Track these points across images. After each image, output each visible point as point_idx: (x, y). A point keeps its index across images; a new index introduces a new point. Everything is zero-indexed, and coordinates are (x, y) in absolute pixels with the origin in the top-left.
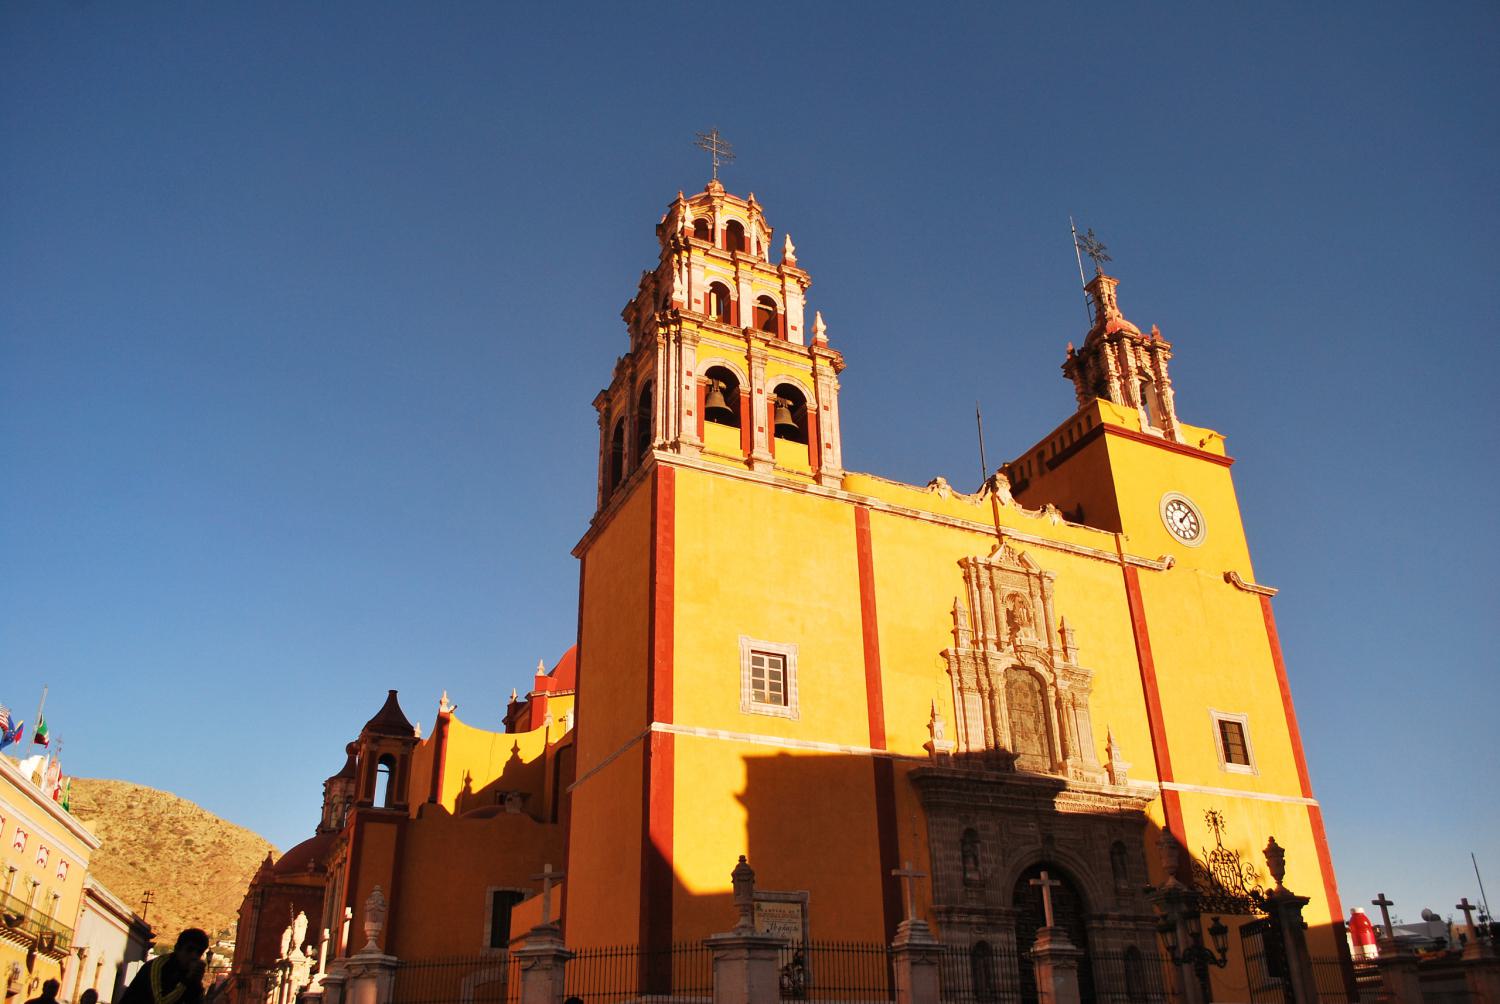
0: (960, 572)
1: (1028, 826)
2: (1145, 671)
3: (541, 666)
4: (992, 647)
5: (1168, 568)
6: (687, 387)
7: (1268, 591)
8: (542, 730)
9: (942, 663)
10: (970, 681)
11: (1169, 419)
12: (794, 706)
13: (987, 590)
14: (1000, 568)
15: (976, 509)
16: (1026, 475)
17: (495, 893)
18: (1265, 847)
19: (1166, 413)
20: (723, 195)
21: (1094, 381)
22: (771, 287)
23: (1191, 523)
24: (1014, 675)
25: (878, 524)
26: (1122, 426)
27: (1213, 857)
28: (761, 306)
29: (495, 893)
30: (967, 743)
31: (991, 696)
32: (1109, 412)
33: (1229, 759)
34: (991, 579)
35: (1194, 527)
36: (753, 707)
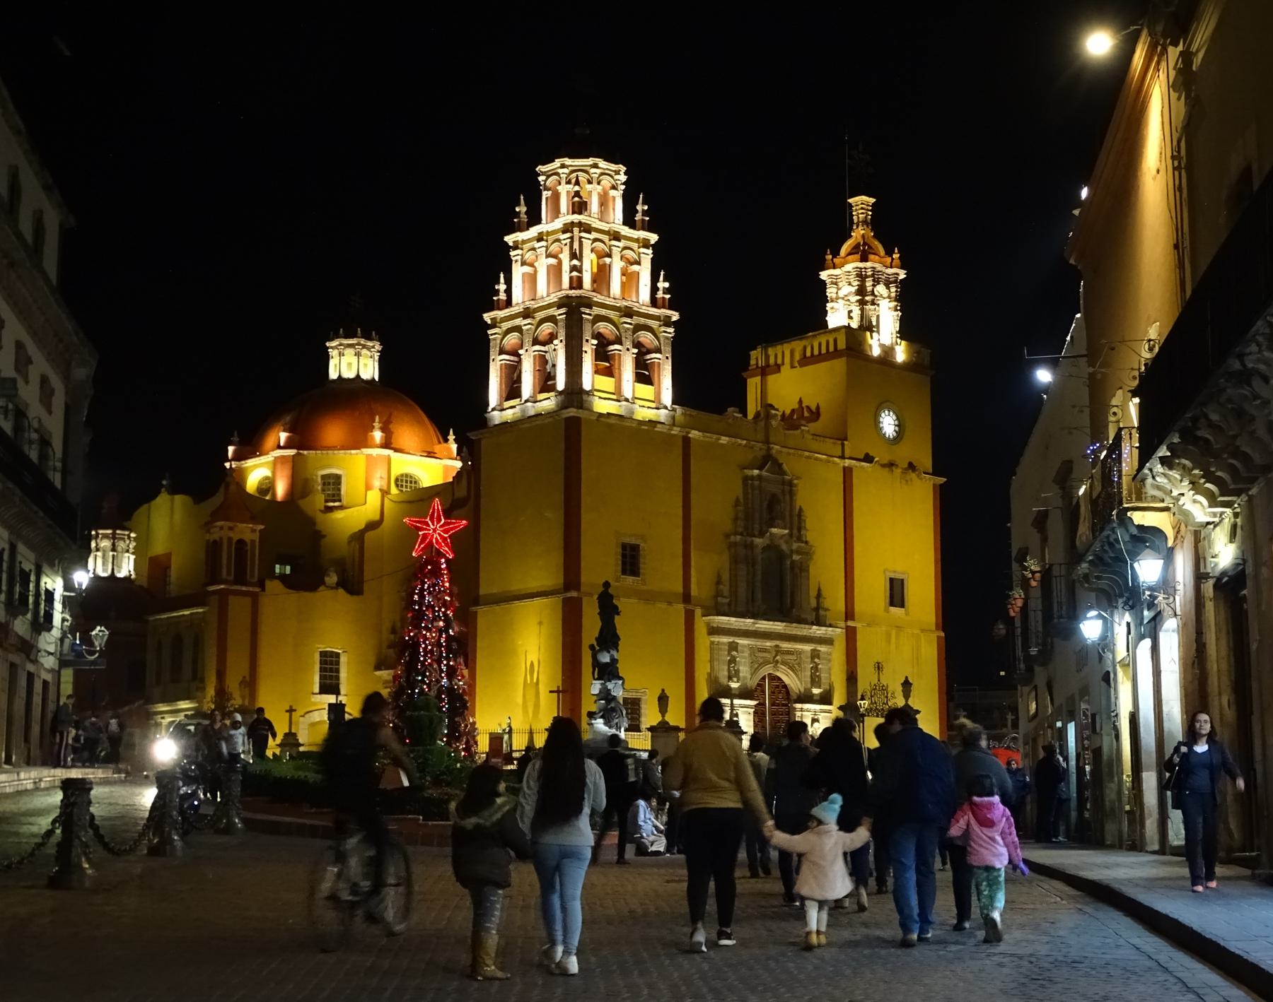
13: (757, 492)
16: (779, 361)
18: (902, 682)
33: (892, 604)
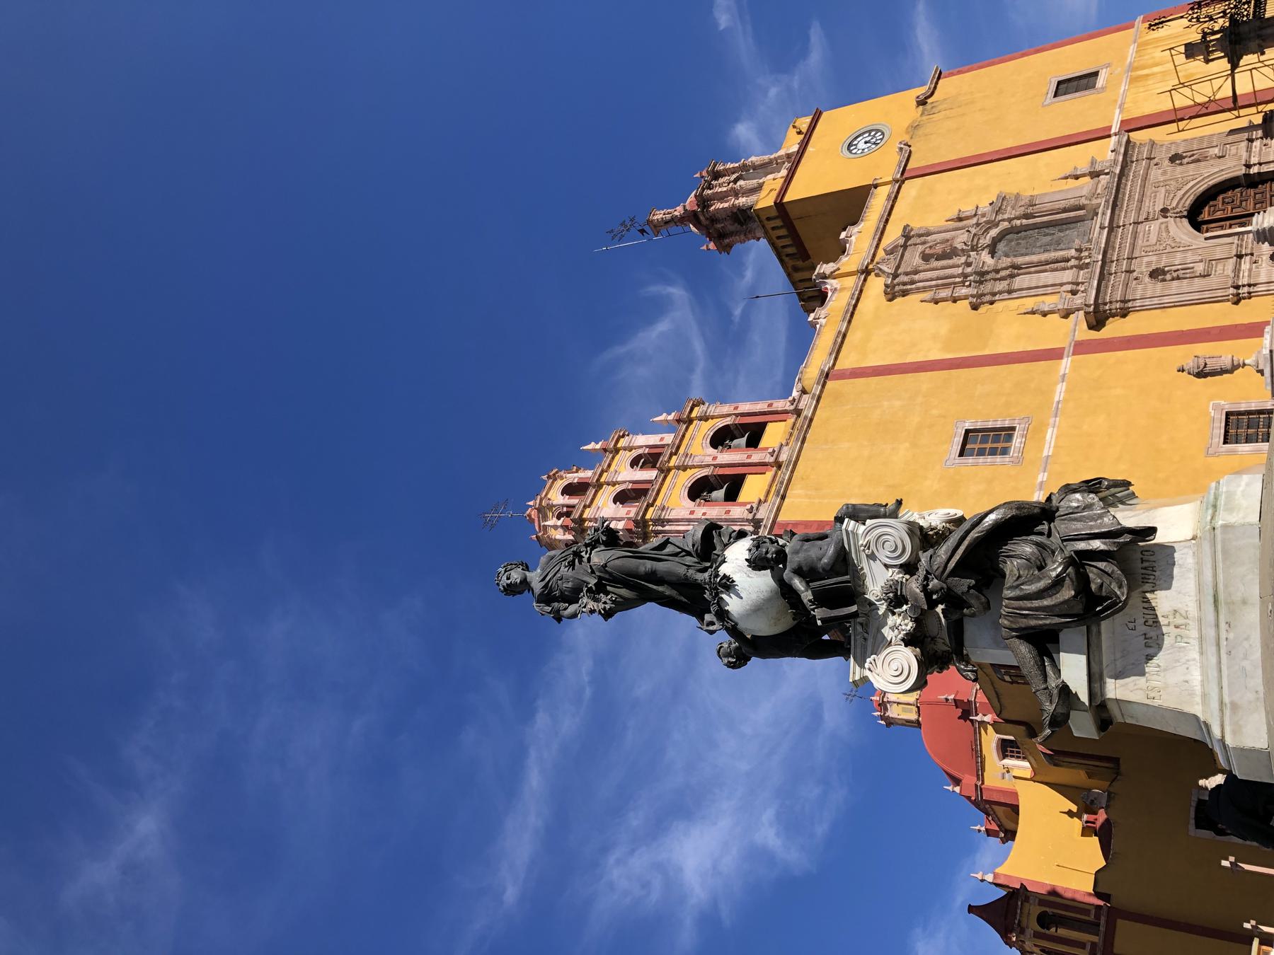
0: (899, 300)
1: (1149, 230)
2: (1002, 156)
3: (950, 788)
4: (969, 270)
5: (910, 146)
6: (704, 514)
7: (936, 72)
8: (1020, 787)
9: (983, 309)
10: (1002, 286)
11: (776, 159)
12: (1016, 421)
13: (916, 277)
14: (898, 267)
15: (839, 293)
17: (1198, 826)
19: (770, 162)
20: (539, 497)
21: (736, 224)
22: (625, 458)
23: (869, 135)
24: (999, 253)
25: (846, 362)
26: (777, 191)
27: (1194, 20)
28: (639, 466)
29: (1198, 826)
30: (1061, 285)
31: (1019, 267)
32: (765, 200)
33: (1094, 86)
34: (907, 274)
35: (873, 133)
36: (1015, 455)
